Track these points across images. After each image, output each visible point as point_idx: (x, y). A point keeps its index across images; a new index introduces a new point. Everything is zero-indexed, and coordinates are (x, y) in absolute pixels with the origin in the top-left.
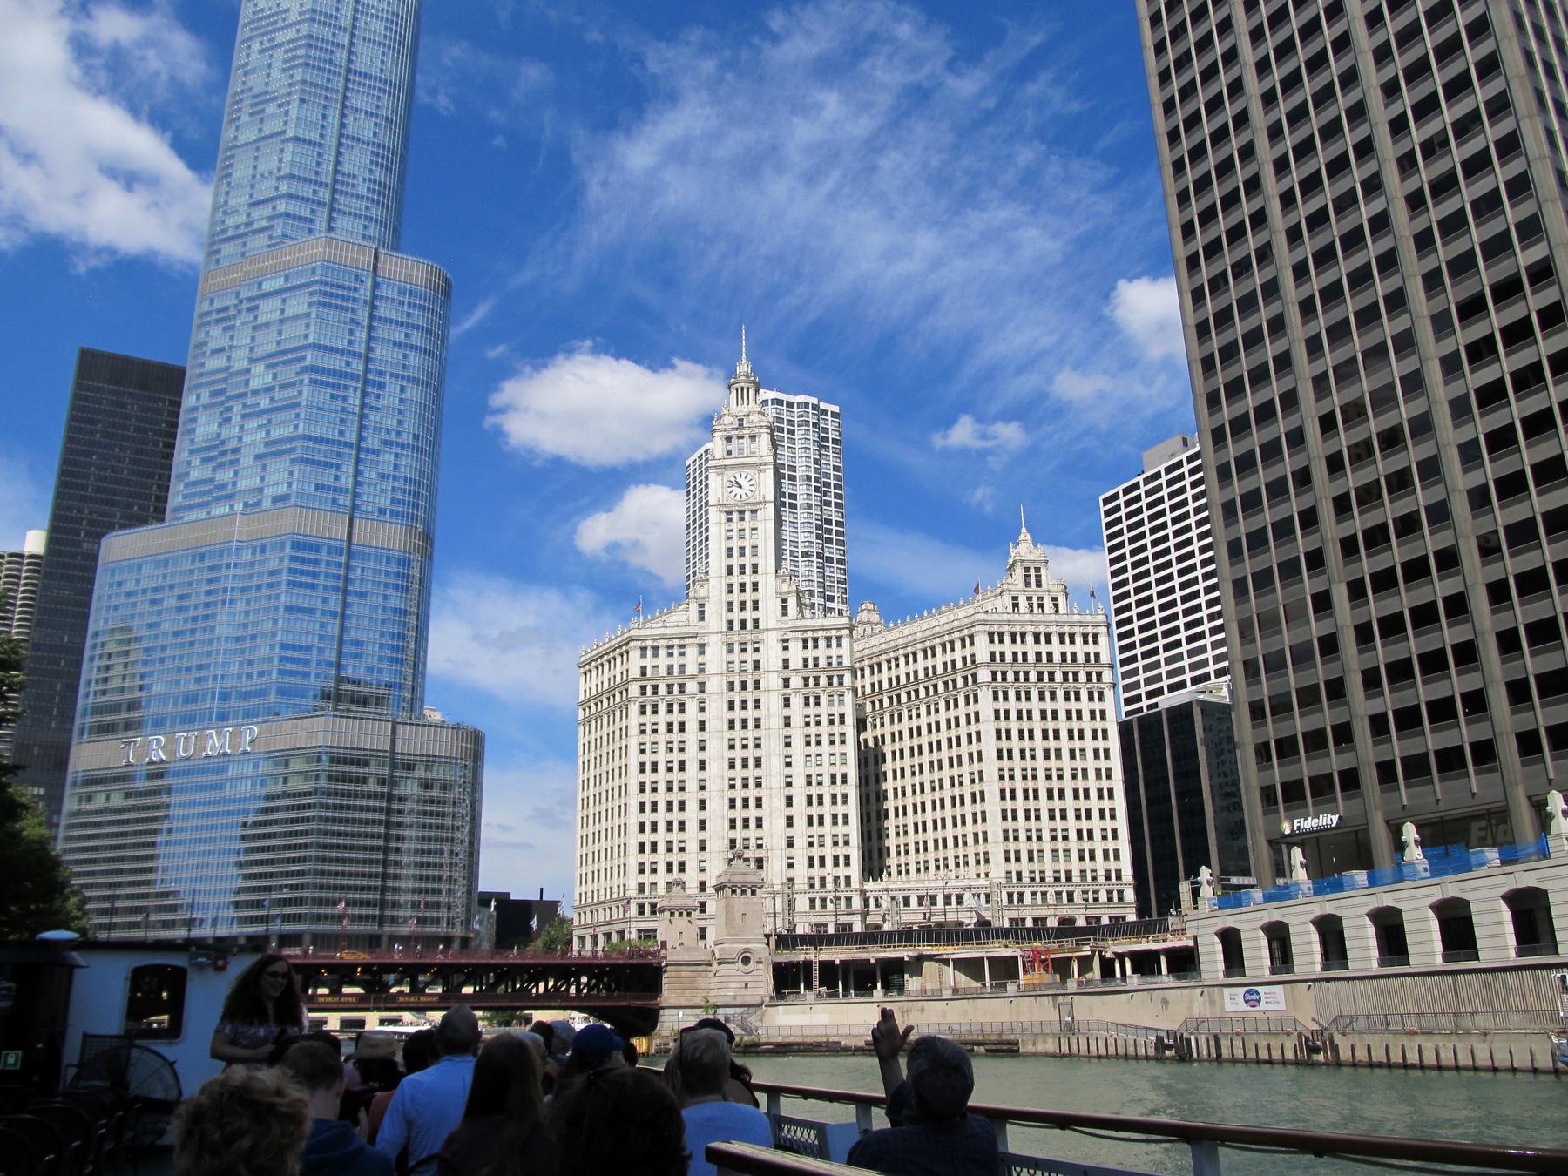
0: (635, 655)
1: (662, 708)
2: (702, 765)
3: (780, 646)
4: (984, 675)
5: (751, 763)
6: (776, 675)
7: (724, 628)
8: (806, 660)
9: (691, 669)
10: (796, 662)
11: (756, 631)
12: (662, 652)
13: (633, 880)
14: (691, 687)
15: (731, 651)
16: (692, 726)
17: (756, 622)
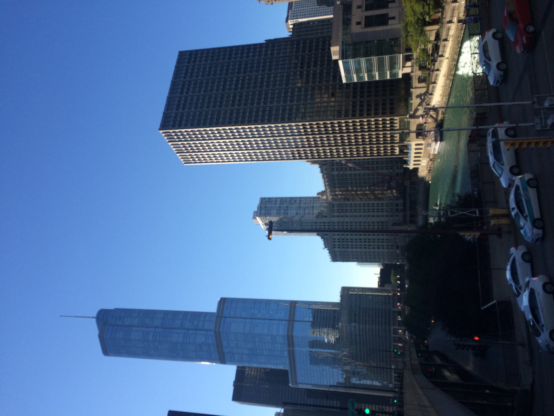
0: (335, 249)
1: (347, 243)
4: (341, 173)
8: (338, 212)
10: (337, 214)
13: (386, 250)
17: (329, 223)
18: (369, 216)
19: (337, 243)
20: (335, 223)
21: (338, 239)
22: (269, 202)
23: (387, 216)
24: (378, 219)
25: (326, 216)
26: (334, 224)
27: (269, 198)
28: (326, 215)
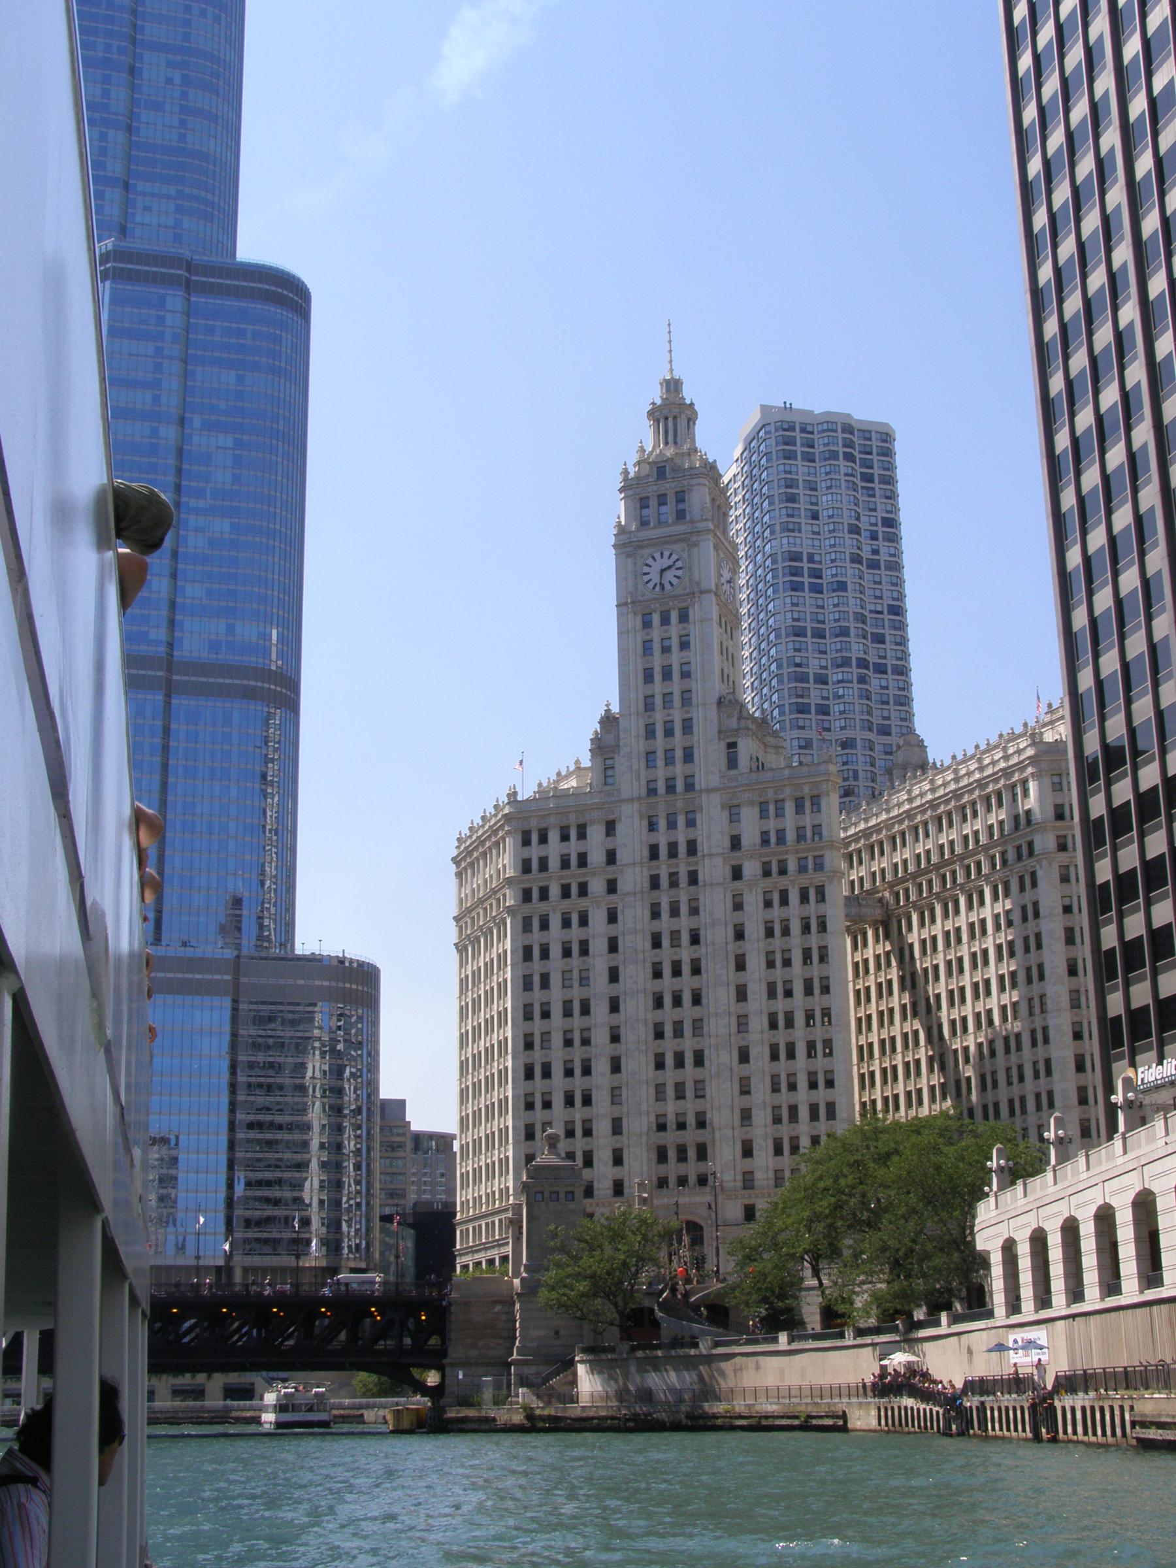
2: (614, 1006)
3: (726, 813)
5: (687, 998)
6: (718, 861)
7: (644, 792)
9: (597, 857)
11: (690, 795)
12: (554, 836)
14: (597, 886)
15: (652, 827)
16: (599, 946)
18: (744, 1057)
19: (554, 849)
20: (691, 823)
21: (583, 860)
22: (868, 478)
23: (748, 1181)
24: (723, 1116)
25: (732, 763)
26: (681, 821)
27: (889, 480)
28: (743, 761)
